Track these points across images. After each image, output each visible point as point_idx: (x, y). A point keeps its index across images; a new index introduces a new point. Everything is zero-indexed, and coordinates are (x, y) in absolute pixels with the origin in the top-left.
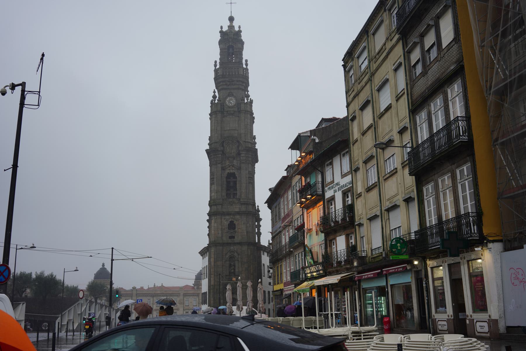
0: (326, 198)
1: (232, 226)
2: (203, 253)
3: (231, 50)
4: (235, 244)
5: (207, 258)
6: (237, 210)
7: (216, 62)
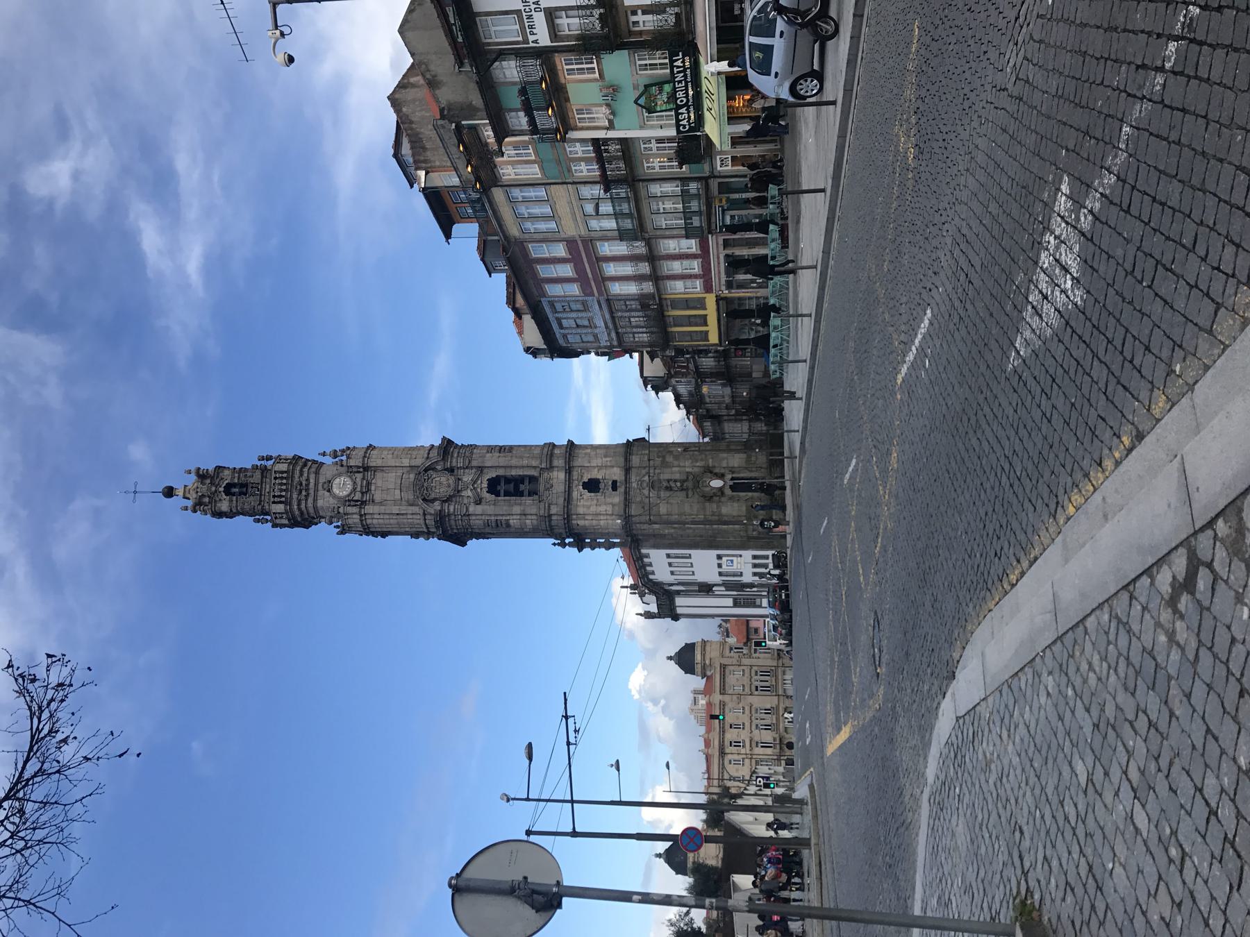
0: (548, 43)
1: (592, 486)
4: (627, 480)
6: (562, 475)
7: (258, 521)
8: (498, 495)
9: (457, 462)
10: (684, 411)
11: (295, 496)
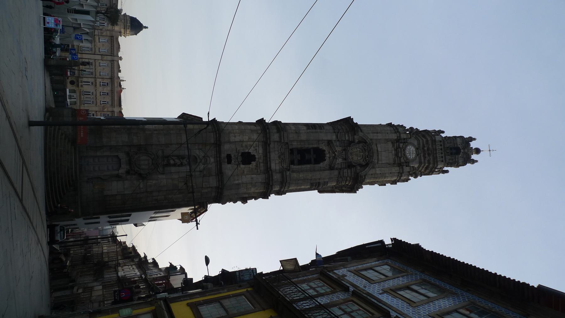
1: (247, 158)
3: (454, 151)
7: (443, 132)
9: (347, 172)
10: (148, 259)
11: (430, 146)
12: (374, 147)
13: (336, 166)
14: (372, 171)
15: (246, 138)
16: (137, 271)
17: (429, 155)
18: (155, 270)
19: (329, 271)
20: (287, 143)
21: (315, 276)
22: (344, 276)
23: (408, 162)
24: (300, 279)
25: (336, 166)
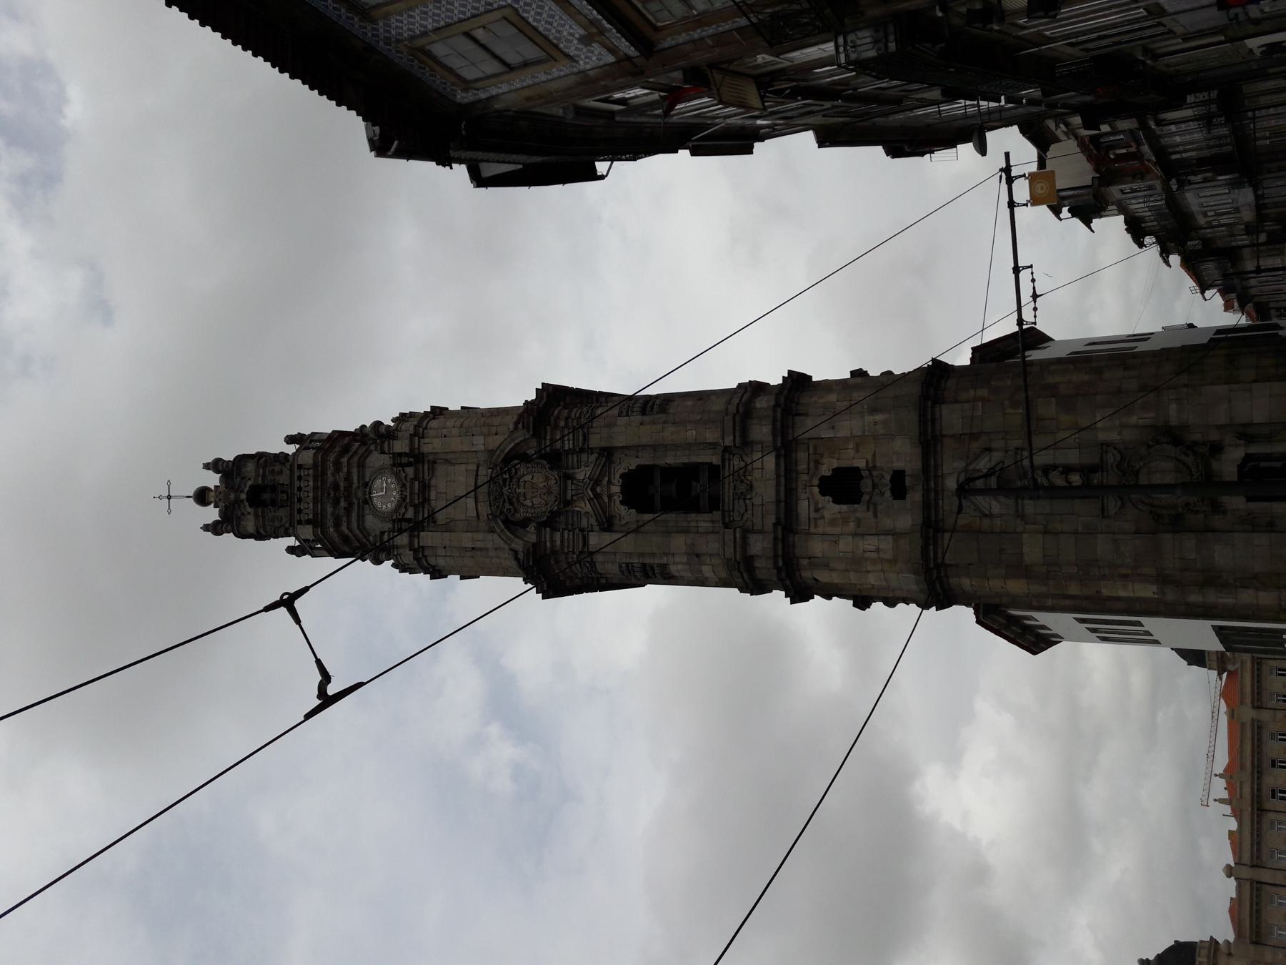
1: (844, 486)
2: (1035, 641)
3: (266, 496)
4: (930, 470)
5: (1043, 618)
7: (291, 550)
8: (641, 510)
11: (330, 510)
12: (484, 510)
13: (593, 458)
14: (494, 442)
15: (846, 545)
16: (1195, 208)
17: (336, 487)
18: (1137, 206)
19: (628, 58)
20: (726, 526)
21: (669, 42)
22: (586, 40)
23: (394, 465)
24: (711, 31)
25: (593, 458)
